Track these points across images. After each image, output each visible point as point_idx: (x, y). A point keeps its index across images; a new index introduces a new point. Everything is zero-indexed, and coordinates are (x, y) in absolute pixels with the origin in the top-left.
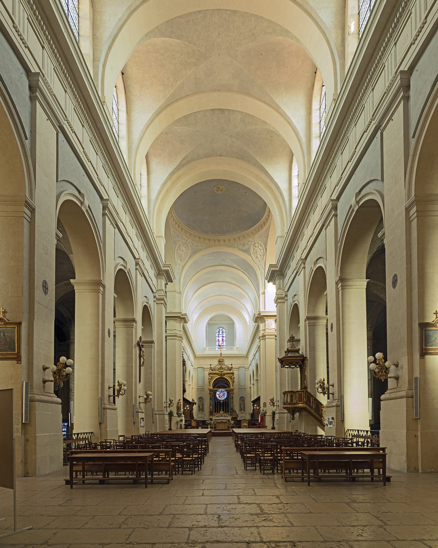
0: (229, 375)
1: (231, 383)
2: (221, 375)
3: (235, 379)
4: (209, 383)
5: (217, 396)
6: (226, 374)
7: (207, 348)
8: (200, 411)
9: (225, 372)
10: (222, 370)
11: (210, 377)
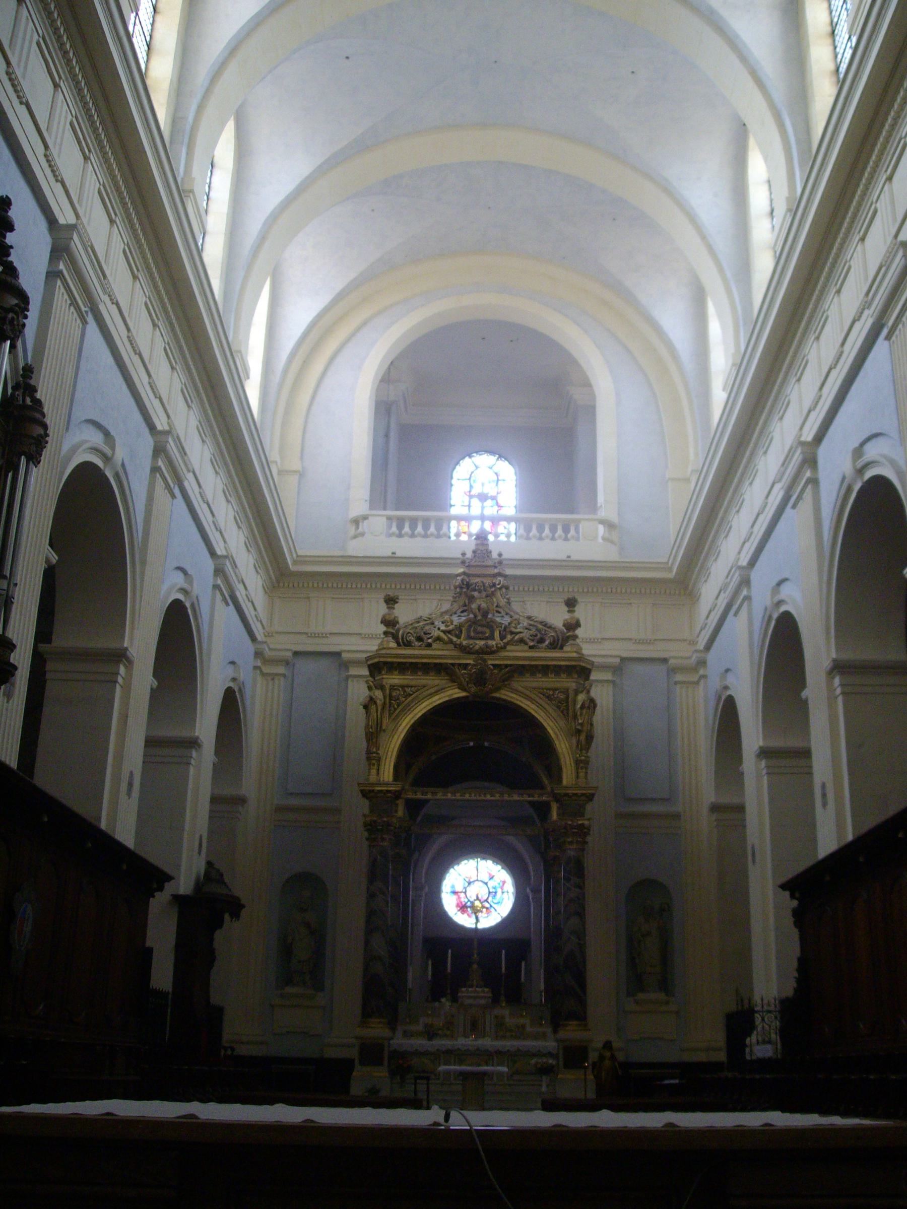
0: (550, 681)
1: (563, 747)
2: (480, 678)
3: (597, 718)
4: (373, 735)
5: (449, 904)
7: (378, 522)
9: (518, 654)
11: (378, 694)
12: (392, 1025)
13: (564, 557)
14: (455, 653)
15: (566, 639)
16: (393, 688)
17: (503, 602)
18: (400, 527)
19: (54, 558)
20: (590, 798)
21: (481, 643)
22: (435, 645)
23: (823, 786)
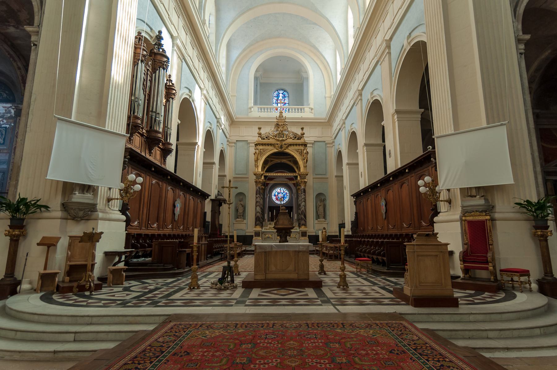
0: (297, 147)
1: (301, 163)
2: (281, 147)
3: (308, 156)
4: (257, 160)
5: (274, 198)
6: (291, 145)
8: (238, 218)
9: (290, 141)
10: (283, 138)
11: (257, 151)
12: (262, 227)
13: (301, 117)
14: (275, 141)
15: (301, 137)
16: (260, 149)
17: (286, 128)
18: (261, 110)
19: (180, 122)
20: (307, 175)
21: (281, 139)
22: (270, 139)
23: (361, 172)
